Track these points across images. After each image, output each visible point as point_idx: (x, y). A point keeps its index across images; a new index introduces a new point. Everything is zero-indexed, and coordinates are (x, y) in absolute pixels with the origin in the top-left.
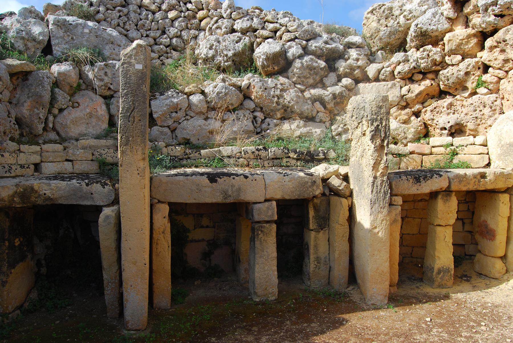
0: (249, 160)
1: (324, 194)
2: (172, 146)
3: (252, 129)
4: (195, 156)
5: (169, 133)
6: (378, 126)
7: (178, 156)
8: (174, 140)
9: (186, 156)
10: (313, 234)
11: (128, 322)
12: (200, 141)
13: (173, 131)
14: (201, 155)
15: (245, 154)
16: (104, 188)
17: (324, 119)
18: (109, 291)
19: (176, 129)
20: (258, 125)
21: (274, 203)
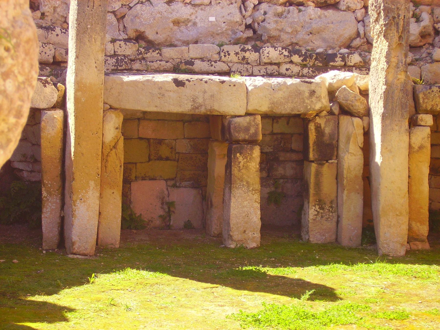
0: (230, 65)
1: (331, 113)
2: (120, 40)
3: (238, 20)
4: (153, 57)
5: (115, 22)
6: (394, 18)
7: (129, 55)
8: (122, 33)
9: (140, 56)
10: (314, 166)
11: (73, 244)
12: (159, 35)
13: (121, 19)
14: (161, 55)
15: (225, 56)
16: (45, 86)
17: (353, 6)
18: (48, 214)
19: (124, 16)
20: (248, 14)
21: (259, 118)
